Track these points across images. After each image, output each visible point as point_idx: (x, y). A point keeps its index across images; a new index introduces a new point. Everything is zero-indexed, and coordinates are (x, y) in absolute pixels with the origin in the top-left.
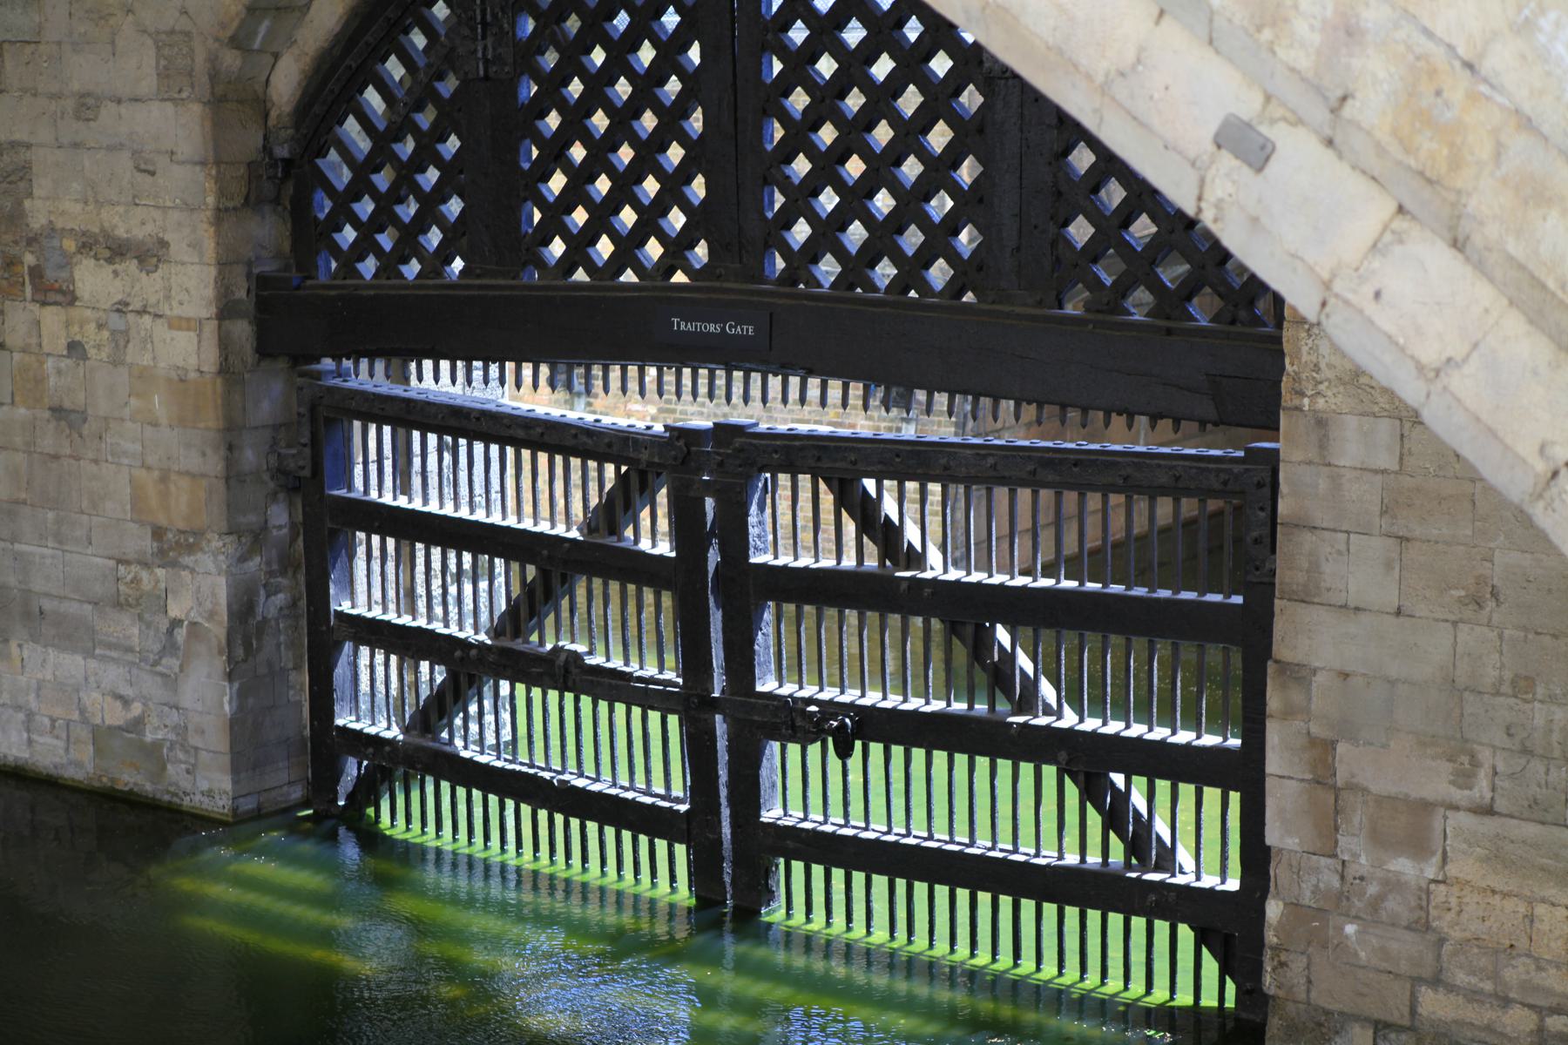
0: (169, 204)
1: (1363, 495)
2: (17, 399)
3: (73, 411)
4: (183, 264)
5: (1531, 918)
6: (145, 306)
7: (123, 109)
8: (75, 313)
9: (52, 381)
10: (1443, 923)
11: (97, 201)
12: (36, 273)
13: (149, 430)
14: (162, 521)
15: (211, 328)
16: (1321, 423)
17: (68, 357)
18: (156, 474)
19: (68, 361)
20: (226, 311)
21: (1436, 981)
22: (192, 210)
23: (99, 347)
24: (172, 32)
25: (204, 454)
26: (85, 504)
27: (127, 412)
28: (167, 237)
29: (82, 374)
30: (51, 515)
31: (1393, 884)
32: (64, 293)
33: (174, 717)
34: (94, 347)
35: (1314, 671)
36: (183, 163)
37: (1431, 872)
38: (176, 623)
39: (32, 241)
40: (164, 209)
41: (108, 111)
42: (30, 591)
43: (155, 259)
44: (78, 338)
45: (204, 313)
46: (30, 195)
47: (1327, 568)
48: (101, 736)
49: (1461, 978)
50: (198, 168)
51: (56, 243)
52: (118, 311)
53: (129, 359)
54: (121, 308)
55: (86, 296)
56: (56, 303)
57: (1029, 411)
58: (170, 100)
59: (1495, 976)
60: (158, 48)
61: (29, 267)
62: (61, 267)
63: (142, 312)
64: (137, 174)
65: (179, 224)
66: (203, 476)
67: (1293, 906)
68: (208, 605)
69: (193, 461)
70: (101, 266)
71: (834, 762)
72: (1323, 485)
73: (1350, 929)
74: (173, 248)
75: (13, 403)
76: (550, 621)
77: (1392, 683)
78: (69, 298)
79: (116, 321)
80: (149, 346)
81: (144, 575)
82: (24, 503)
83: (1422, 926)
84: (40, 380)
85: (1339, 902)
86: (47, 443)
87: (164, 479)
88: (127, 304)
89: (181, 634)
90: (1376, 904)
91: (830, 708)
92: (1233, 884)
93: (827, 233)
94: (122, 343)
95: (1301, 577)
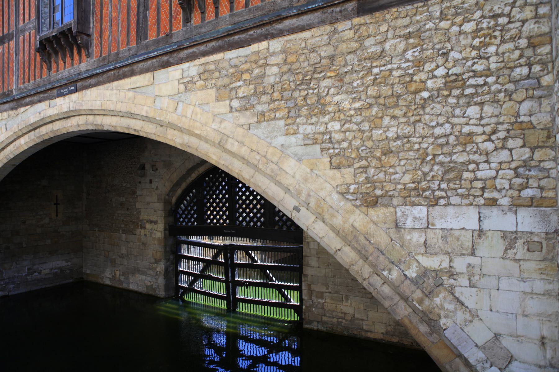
1: (313, 252)
5: (336, 307)
9: (142, 239)
10: (325, 308)
12: (141, 225)
15: (163, 232)
16: (308, 243)
20: (165, 229)
21: (325, 315)
31: (319, 303)
33: (157, 284)
38: (158, 271)
47: (309, 262)
49: (328, 315)
54: (151, 229)
57: (271, 242)
63: (154, 230)
67: (306, 306)
71: (246, 289)
72: (309, 251)
73: (314, 309)
76: (207, 271)
77: (318, 276)
78: (145, 228)
79: (151, 231)
83: (323, 308)
85: (312, 306)
86: (141, 248)
89: (158, 273)
90: (317, 305)
91: (245, 282)
92: (299, 304)
93: (244, 219)
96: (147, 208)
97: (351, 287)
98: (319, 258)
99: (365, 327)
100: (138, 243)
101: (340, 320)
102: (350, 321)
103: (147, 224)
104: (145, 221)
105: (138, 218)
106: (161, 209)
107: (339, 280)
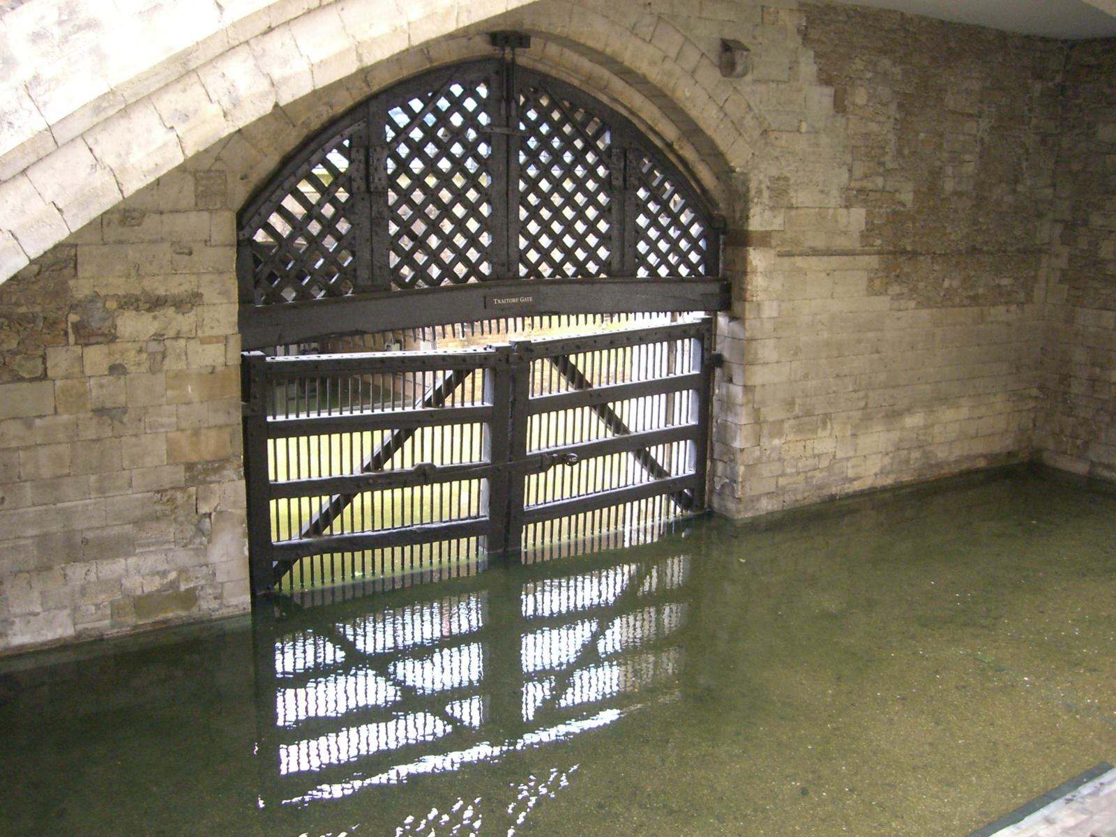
0: (202, 271)
1: (769, 326)
2: (60, 410)
3: (115, 408)
4: (214, 305)
6: (179, 332)
7: (165, 218)
8: (117, 347)
9: (94, 393)
11: (139, 275)
12: (77, 327)
13: (183, 409)
14: (193, 458)
18: (189, 432)
21: (783, 475)
22: (221, 273)
23: (139, 365)
24: (209, 171)
25: (229, 413)
26: (126, 463)
27: (164, 399)
28: (200, 291)
30: (93, 478)
31: (774, 449)
34: (134, 365)
35: (755, 387)
36: (215, 246)
37: (783, 441)
39: (73, 307)
40: (198, 274)
41: (150, 222)
42: (74, 530)
43: (190, 305)
44: (118, 362)
45: (230, 332)
46: (75, 276)
48: (141, 603)
49: (789, 471)
50: (228, 248)
51: (100, 305)
52: (154, 340)
53: (165, 368)
54: (159, 337)
55: (127, 335)
56: (97, 343)
58: (208, 210)
59: (796, 466)
60: (196, 179)
61: (72, 324)
62: (104, 320)
63: (177, 337)
64: (177, 257)
65: (211, 282)
66: (228, 425)
67: (748, 466)
68: (232, 499)
69: (221, 419)
72: (758, 324)
74: (206, 298)
75: (56, 412)
77: (775, 384)
78: (111, 338)
79: (154, 346)
80: (184, 357)
81: (179, 495)
82: (69, 475)
83: (779, 459)
84: (83, 395)
86: (91, 434)
87: (196, 432)
88: (163, 335)
94: (159, 357)
95: (752, 356)
96: (121, 242)
97: (834, 392)
99: (851, 473)
100: (65, 417)
101: (809, 474)
102: (829, 468)
103: (127, 314)
104: (112, 305)
105: (61, 291)
106: (217, 238)
107: (814, 382)
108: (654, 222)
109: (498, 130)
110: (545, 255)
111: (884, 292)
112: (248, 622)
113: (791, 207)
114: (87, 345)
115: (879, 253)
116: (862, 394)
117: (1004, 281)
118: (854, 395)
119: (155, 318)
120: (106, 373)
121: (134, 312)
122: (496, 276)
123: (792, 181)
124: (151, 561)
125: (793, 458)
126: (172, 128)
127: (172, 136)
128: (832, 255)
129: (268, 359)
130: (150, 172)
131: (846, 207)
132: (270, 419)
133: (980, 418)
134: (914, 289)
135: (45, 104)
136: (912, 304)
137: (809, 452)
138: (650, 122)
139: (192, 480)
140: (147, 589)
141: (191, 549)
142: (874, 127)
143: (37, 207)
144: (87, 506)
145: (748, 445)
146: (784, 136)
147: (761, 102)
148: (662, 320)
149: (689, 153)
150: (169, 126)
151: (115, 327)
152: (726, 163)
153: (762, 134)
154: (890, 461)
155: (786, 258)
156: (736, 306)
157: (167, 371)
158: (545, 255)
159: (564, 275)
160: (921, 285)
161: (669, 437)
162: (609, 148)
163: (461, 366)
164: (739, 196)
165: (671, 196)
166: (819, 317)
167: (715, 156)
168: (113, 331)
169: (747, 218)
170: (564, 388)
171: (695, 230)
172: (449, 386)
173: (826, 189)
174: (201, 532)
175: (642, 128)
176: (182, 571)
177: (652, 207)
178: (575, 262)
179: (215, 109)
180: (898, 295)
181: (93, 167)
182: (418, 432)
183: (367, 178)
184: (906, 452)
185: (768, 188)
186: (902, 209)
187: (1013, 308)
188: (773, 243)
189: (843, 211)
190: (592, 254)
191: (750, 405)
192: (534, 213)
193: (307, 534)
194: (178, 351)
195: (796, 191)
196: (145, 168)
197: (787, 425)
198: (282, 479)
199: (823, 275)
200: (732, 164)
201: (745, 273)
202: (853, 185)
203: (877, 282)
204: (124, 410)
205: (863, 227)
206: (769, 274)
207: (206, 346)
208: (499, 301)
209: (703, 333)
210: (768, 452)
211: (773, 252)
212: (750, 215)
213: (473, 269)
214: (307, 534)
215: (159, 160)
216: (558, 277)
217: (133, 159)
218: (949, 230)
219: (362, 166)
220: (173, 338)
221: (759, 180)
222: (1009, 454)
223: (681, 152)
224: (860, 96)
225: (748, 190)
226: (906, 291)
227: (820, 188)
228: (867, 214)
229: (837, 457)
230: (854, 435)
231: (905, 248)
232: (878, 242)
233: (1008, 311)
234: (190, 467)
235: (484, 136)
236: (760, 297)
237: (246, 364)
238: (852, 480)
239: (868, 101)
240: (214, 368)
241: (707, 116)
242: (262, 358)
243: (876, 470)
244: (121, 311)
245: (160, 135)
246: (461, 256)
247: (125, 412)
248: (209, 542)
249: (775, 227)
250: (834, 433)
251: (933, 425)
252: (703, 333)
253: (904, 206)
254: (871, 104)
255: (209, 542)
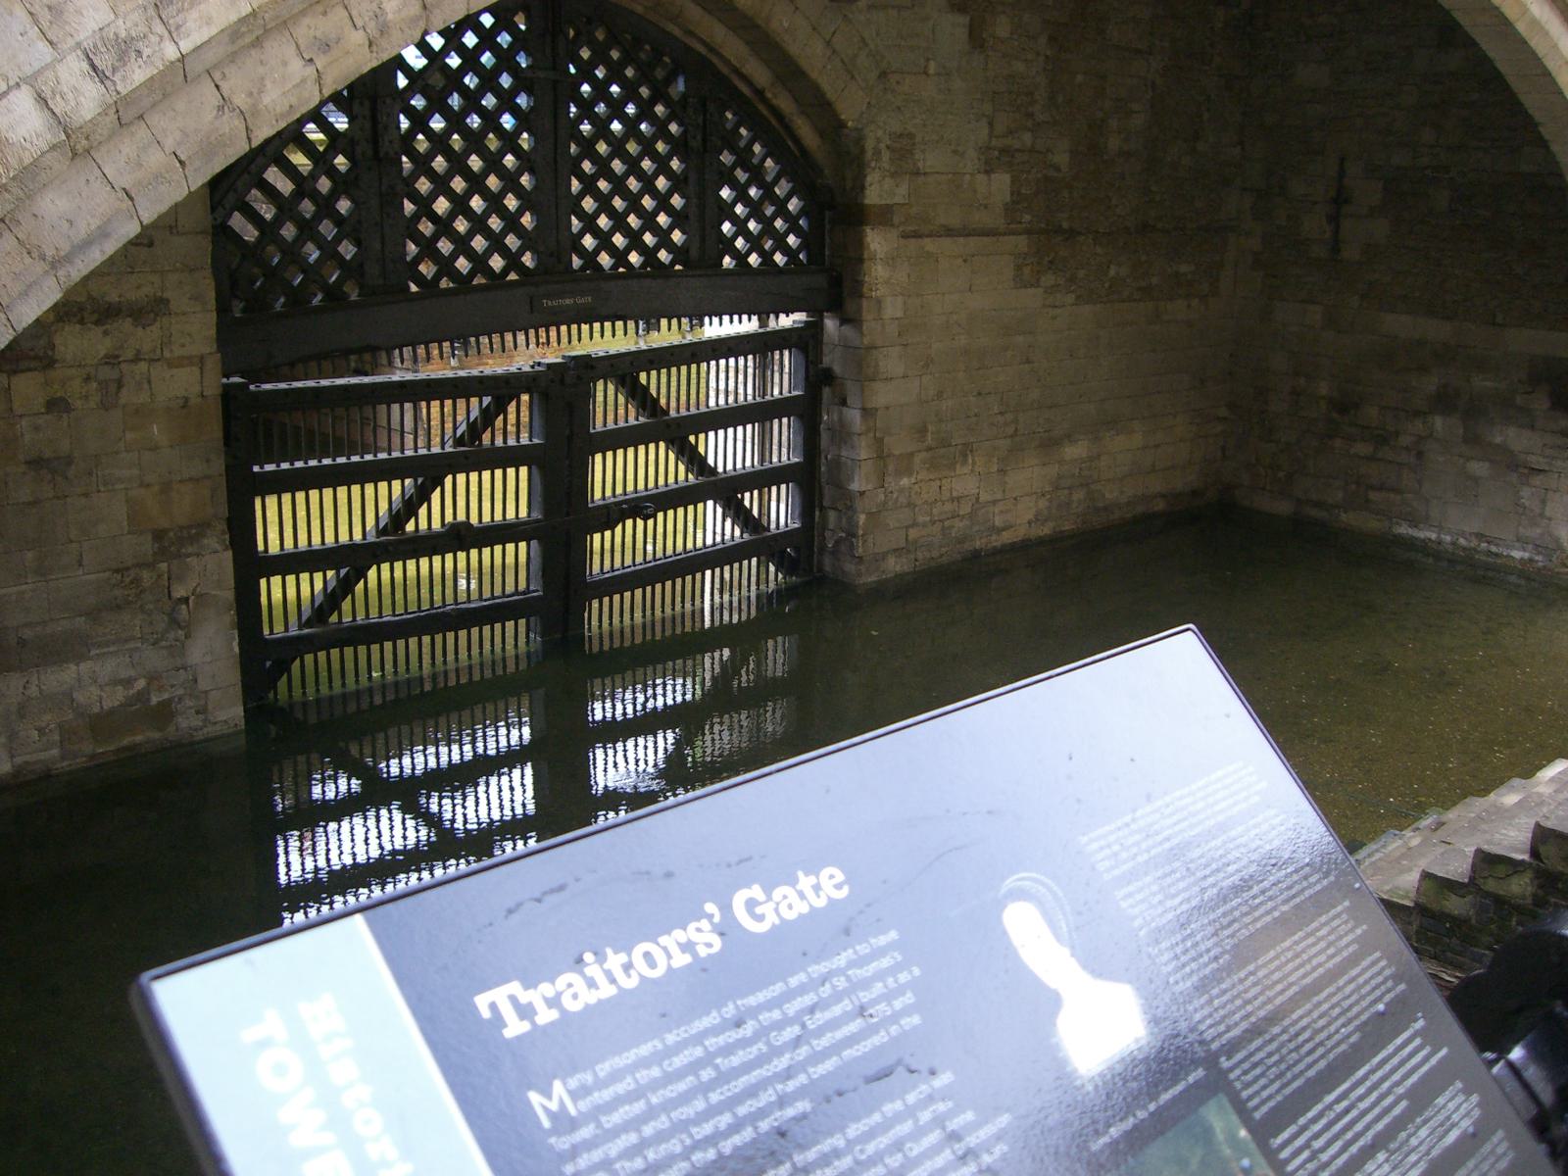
0: (167, 268)
9: (27, 438)
17: (47, 413)
18: (156, 488)
19: (48, 417)
21: (914, 524)
28: (165, 295)
29: (65, 423)
30: (30, 555)
31: (901, 490)
32: (36, 358)
34: (80, 398)
35: (877, 410)
37: (913, 481)
38: (186, 600)
43: (152, 315)
49: (921, 519)
52: (106, 363)
53: (122, 401)
54: (112, 360)
59: (931, 514)
63: (137, 359)
67: (870, 514)
70: (90, 329)
79: (107, 373)
80: (146, 386)
81: (145, 575)
87: (166, 488)
88: (117, 357)
94: (113, 388)
98: (905, 345)
99: (998, 522)
101: (947, 523)
102: (972, 515)
108: (742, 196)
109: (541, 74)
110: (604, 241)
111: (1036, 284)
112: (242, 741)
113: (917, 173)
114: (15, 372)
115: (1028, 232)
116: (1009, 417)
117: (1184, 268)
118: (1000, 418)
119: (106, 333)
120: (43, 410)
121: (78, 326)
122: (542, 269)
123: (918, 139)
124: (108, 667)
125: (926, 502)
126: (311, 60)
127: (310, 71)
128: (968, 235)
129: (252, 387)
130: (283, 116)
131: (987, 172)
132: (256, 469)
133: (1157, 446)
134: (1072, 280)
135: (178, 27)
136: (1070, 299)
137: (946, 495)
138: (734, 62)
139: (162, 553)
140: (107, 704)
141: (163, 648)
142: (1019, 67)
143: (156, 159)
144: (23, 592)
145: (870, 487)
146: (907, 81)
147: (878, 35)
148: (748, 325)
149: (784, 103)
150: (307, 58)
151: (53, 347)
152: (835, 115)
153: (879, 77)
154: (1047, 504)
155: (913, 240)
156: (850, 306)
157: (124, 406)
158: (604, 241)
159: (628, 265)
160: (1081, 273)
161: (762, 479)
162: (684, 97)
163: (503, 390)
164: (850, 156)
165: (763, 160)
166: (955, 317)
167: (820, 107)
168: (50, 353)
169: (863, 188)
170: (631, 417)
171: (793, 205)
172: (487, 418)
173: (960, 149)
174: (175, 623)
175: (725, 70)
176: (153, 678)
177: (741, 176)
178: (643, 249)
179: (357, 38)
180: (1053, 286)
181: (220, 108)
182: (449, 480)
183: (375, 140)
184: (1066, 492)
185: (888, 147)
186: (1056, 174)
187: (1195, 302)
188: (896, 220)
189: (981, 178)
190: (664, 240)
191: (872, 435)
192: (589, 186)
193: (309, 623)
194: (138, 378)
195: (923, 151)
196: (278, 110)
197: (917, 459)
198: (274, 549)
199: (960, 260)
200: (843, 117)
201: (861, 260)
202: (994, 142)
203: (1027, 270)
204: (69, 461)
205: (1008, 199)
206: (891, 261)
207: (175, 371)
208: (550, 303)
209: (804, 341)
210: (895, 496)
211: (894, 234)
212: (867, 184)
213: (513, 260)
214: (309, 623)
215: (294, 101)
216: (621, 270)
217: (267, 100)
218: (1114, 202)
219: (368, 125)
220: (132, 361)
221: (876, 138)
222: (1194, 493)
223: (775, 102)
224: (1002, 27)
225: (863, 151)
226: (1062, 282)
227: (953, 147)
228: (1012, 182)
229: (981, 500)
230: (1002, 471)
231: (1060, 226)
232: (1027, 217)
233: (1189, 306)
234: (159, 535)
235: (522, 82)
236: (881, 291)
237: (228, 395)
238: (1000, 531)
239: (1012, 34)
240: (186, 399)
241: (809, 52)
242: (245, 386)
243: (1030, 516)
244: (61, 324)
245: (296, 66)
246: (496, 243)
247: (69, 464)
248: (187, 636)
249: (898, 200)
250: (977, 469)
251: (1099, 456)
252: (804, 341)
253: (1058, 169)
254: (1015, 37)
255: (187, 636)
